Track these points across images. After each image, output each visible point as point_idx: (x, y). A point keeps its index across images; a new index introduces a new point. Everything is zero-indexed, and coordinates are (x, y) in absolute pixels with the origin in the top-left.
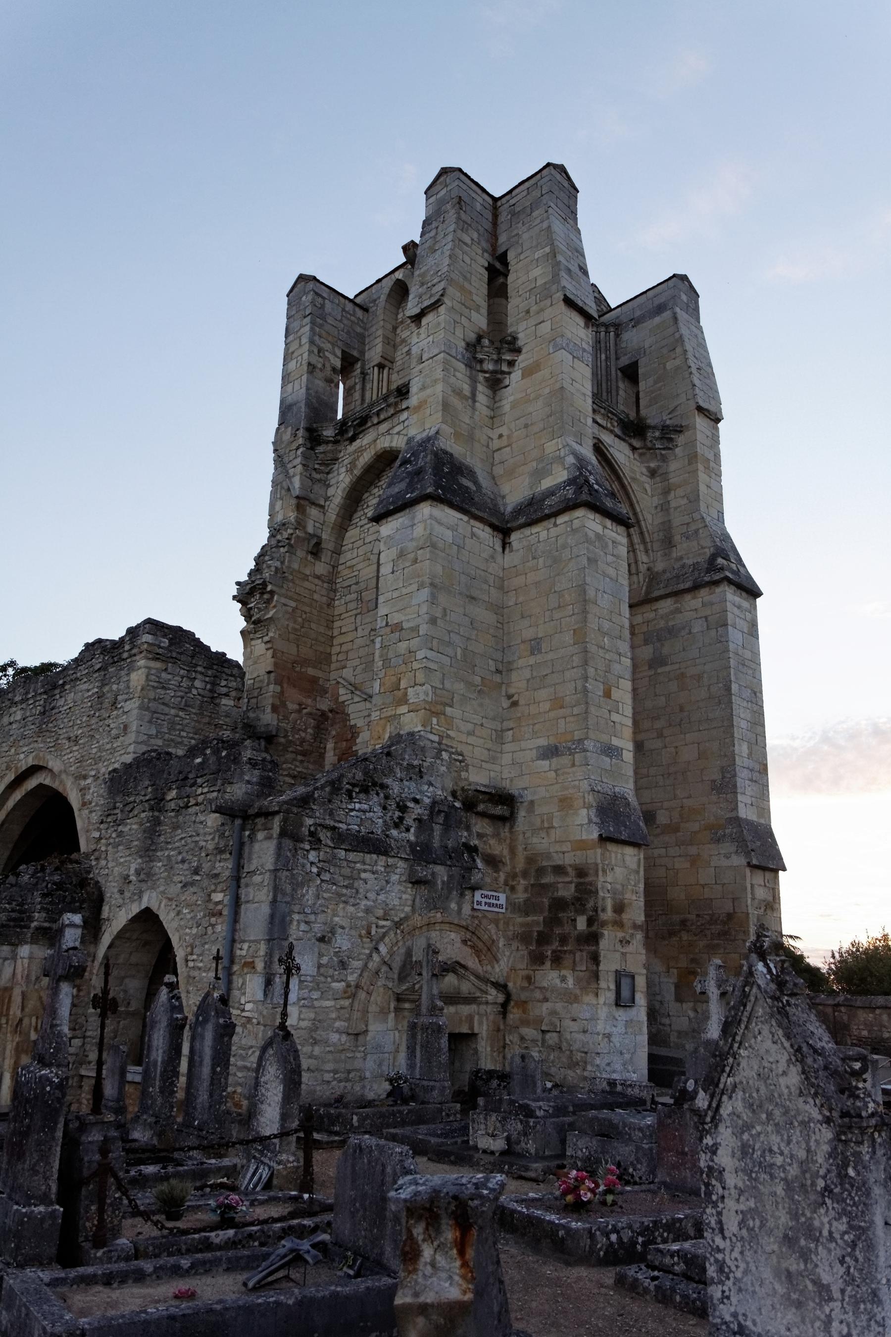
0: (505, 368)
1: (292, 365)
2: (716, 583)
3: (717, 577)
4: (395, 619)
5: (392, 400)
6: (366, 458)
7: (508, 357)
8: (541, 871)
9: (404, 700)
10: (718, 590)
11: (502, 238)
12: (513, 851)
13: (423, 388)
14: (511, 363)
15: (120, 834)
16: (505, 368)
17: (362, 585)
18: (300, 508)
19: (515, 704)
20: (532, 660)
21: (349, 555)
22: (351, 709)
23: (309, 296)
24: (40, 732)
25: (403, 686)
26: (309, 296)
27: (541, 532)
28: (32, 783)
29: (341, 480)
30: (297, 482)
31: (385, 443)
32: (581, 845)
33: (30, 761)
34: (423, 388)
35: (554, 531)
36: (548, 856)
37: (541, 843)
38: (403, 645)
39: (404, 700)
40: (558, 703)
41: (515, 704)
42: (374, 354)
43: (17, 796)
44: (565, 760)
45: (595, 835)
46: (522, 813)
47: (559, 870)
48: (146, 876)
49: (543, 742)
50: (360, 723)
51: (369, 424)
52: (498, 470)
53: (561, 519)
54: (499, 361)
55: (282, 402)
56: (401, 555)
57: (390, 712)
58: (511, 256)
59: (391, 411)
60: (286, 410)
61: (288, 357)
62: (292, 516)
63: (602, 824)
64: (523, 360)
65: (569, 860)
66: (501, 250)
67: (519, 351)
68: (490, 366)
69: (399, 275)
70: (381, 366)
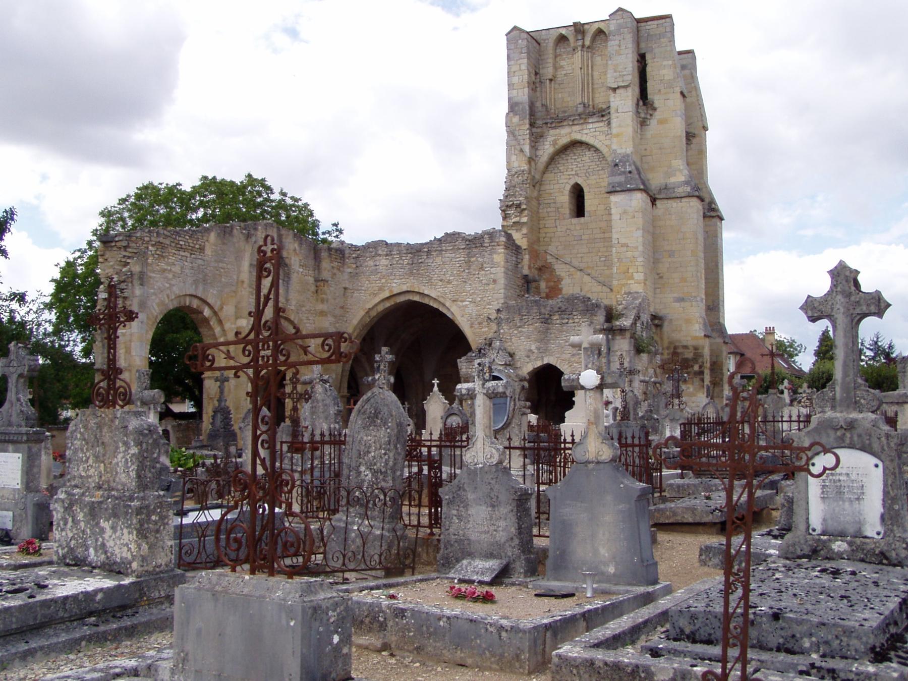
0: (648, 117)
1: (515, 80)
2: (713, 217)
3: (713, 214)
4: (623, 241)
5: (583, 116)
6: (564, 141)
7: (651, 112)
8: (675, 348)
9: (632, 278)
10: (714, 220)
11: (643, 45)
12: (662, 339)
13: (620, 126)
14: (651, 115)
15: (521, 332)
16: (648, 117)
17: (559, 205)
18: (529, 163)
19: (661, 277)
20: (669, 260)
21: (547, 187)
22: (556, 267)
23: (515, 34)
24: (411, 273)
25: (630, 271)
26: (515, 34)
27: (674, 204)
28: (402, 299)
29: (547, 149)
30: (527, 148)
31: (578, 137)
32: (696, 338)
33: (405, 288)
34: (620, 126)
35: (680, 205)
36: (680, 341)
37: (676, 336)
38: (629, 254)
39: (632, 278)
40: (683, 280)
41: (661, 277)
42: (548, 71)
43: (388, 304)
44: (687, 304)
45: (703, 335)
46: (666, 324)
47: (686, 347)
48: (543, 351)
49: (676, 295)
50: (563, 274)
51: (565, 123)
52: (645, 166)
53: (683, 200)
54: (647, 113)
55: (509, 99)
56: (625, 212)
57: (624, 282)
58: (648, 57)
59: (582, 121)
60: (513, 107)
61: (510, 74)
62: (525, 167)
63: (705, 330)
64: (657, 115)
65: (690, 343)
66: (643, 52)
67: (655, 109)
68: (643, 115)
69: (564, 32)
70: (551, 80)
